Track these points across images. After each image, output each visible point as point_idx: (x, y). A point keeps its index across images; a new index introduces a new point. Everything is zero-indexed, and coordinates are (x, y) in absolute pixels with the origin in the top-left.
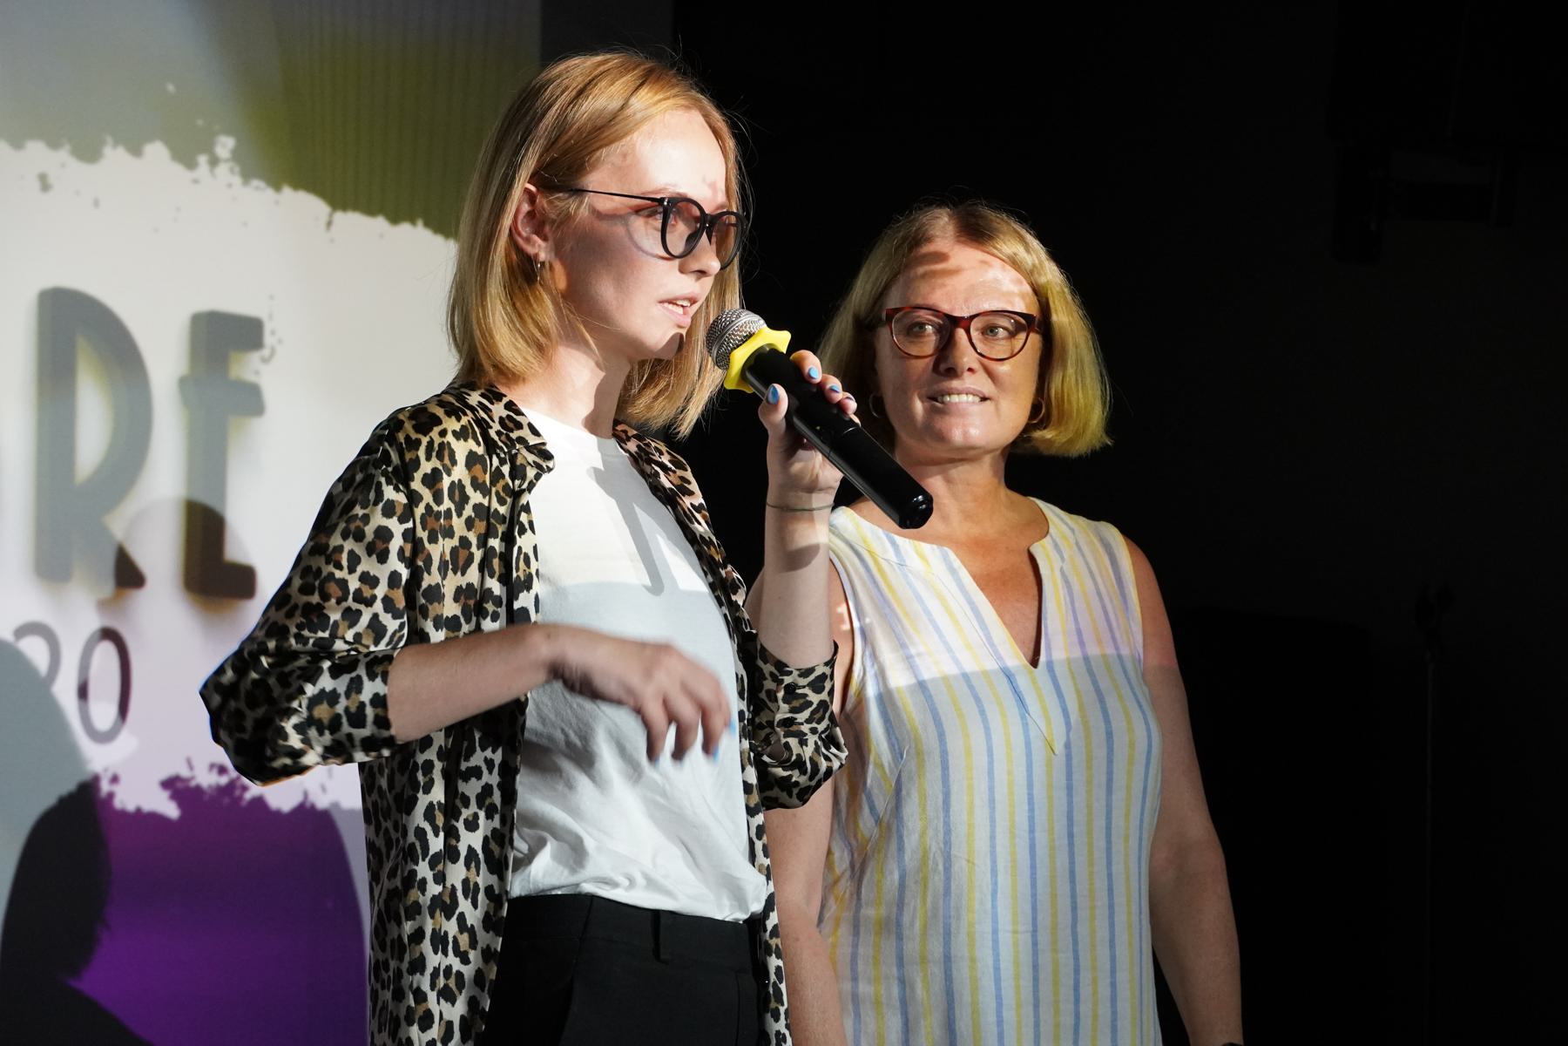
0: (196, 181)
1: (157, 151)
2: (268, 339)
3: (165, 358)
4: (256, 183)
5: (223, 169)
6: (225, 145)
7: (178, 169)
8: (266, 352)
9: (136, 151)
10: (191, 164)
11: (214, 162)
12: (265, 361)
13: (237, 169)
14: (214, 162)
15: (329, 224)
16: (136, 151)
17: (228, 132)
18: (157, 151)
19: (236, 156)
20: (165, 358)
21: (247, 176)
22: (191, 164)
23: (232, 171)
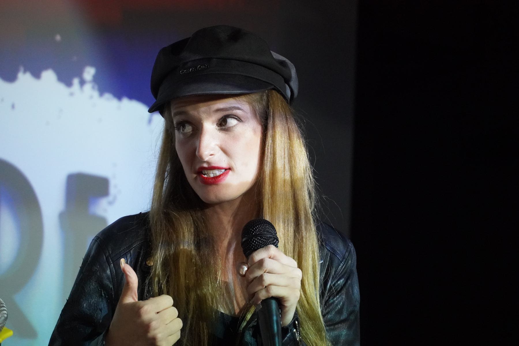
0: (72, 94)
1: (49, 76)
2: (112, 190)
3: (51, 200)
4: (107, 96)
5: (88, 87)
6: (89, 73)
7: (61, 87)
8: (110, 198)
9: (37, 75)
10: (69, 84)
11: (82, 83)
12: (111, 203)
13: (96, 87)
14: (82, 83)
15: (150, 121)
16: (37, 75)
17: (92, 65)
18: (49, 76)
19: (96, 79)
20: (51, 200)
21: (102, 92)
22: (69, 84)
23: (93, 88)
